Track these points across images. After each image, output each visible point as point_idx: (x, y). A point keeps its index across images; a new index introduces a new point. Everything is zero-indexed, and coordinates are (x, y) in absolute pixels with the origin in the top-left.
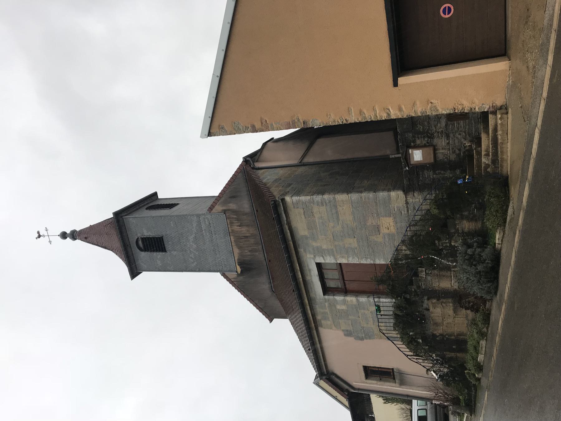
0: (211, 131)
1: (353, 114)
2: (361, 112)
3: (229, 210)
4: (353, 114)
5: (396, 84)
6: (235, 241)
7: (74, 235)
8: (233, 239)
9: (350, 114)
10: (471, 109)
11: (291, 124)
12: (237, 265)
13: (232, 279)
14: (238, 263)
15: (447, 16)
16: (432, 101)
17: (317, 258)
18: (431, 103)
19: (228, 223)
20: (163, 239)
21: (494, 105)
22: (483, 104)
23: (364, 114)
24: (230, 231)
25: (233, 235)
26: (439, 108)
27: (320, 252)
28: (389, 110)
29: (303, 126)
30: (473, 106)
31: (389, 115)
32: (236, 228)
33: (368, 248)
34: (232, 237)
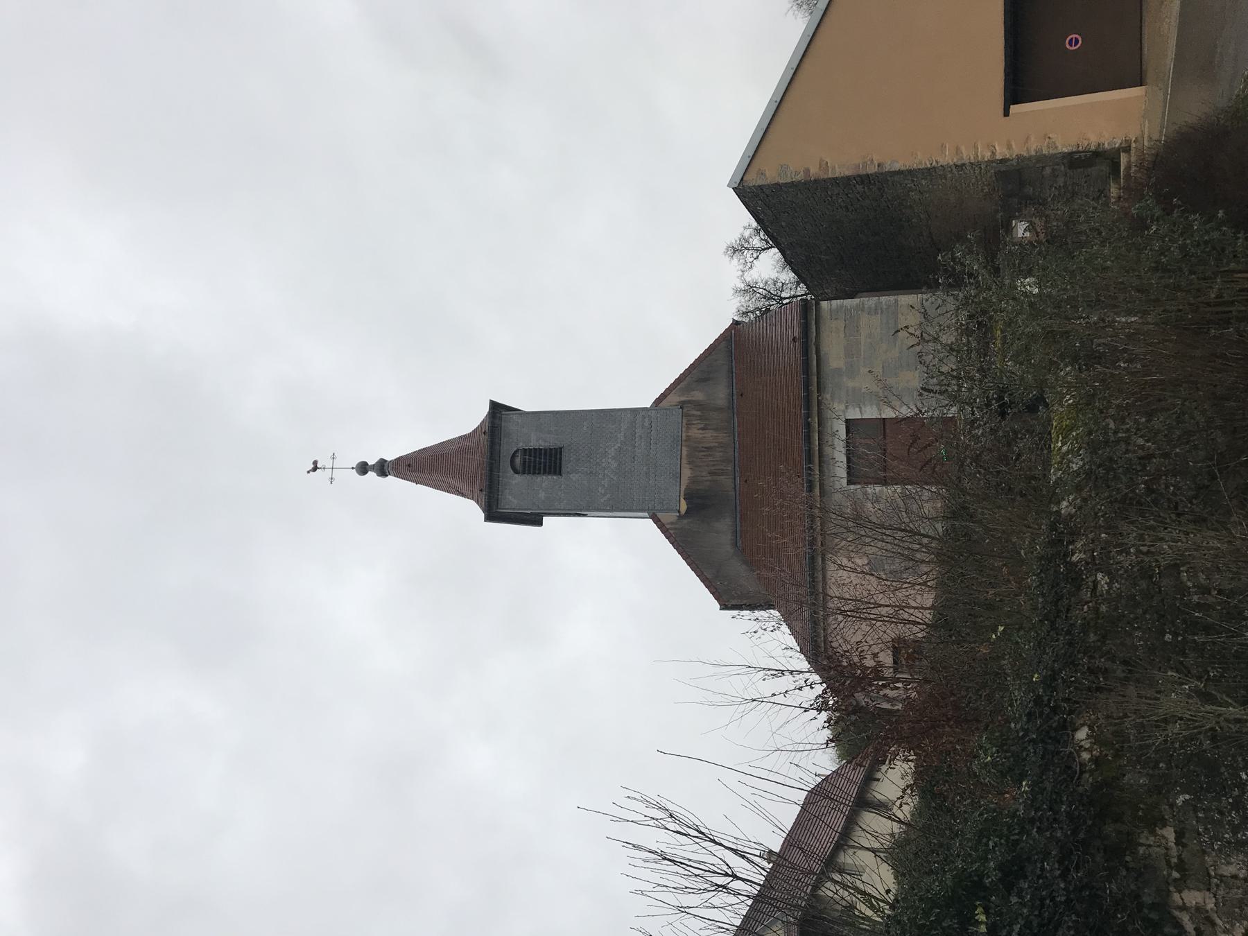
0: (745, 179)
1: (947, 153)
2: (958, 149)
3: (689, 402)
4: (947, 153)
5: (1006, 113)
6: (687, 455)
7: (383, 468)
8: (685, 452)
9: (942, 153)
10: (1099, 144)
11: (861, 167)
12: (682, 499)
13: (668, 524)
14: (685, 495)
15: (1074, 48)
16: (1051, 136)
17: (849, 410)
18: (1049, 138)
19: (684, 424)
20: (561, 452)
21: (1127, 139)
22: (1114, 138)
23: (962, 153)
24: (684, 438)
25: (686, 446)
26: (1058, 144)
27: (858, 399)
28: (994, 147)
29: (876, 170)
30: (1102, 140)
31: (993, 153)
32: (695, 432)
33: (866, 658)
34: (684, 449)
